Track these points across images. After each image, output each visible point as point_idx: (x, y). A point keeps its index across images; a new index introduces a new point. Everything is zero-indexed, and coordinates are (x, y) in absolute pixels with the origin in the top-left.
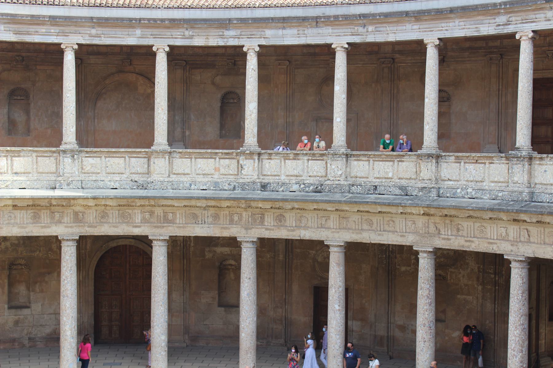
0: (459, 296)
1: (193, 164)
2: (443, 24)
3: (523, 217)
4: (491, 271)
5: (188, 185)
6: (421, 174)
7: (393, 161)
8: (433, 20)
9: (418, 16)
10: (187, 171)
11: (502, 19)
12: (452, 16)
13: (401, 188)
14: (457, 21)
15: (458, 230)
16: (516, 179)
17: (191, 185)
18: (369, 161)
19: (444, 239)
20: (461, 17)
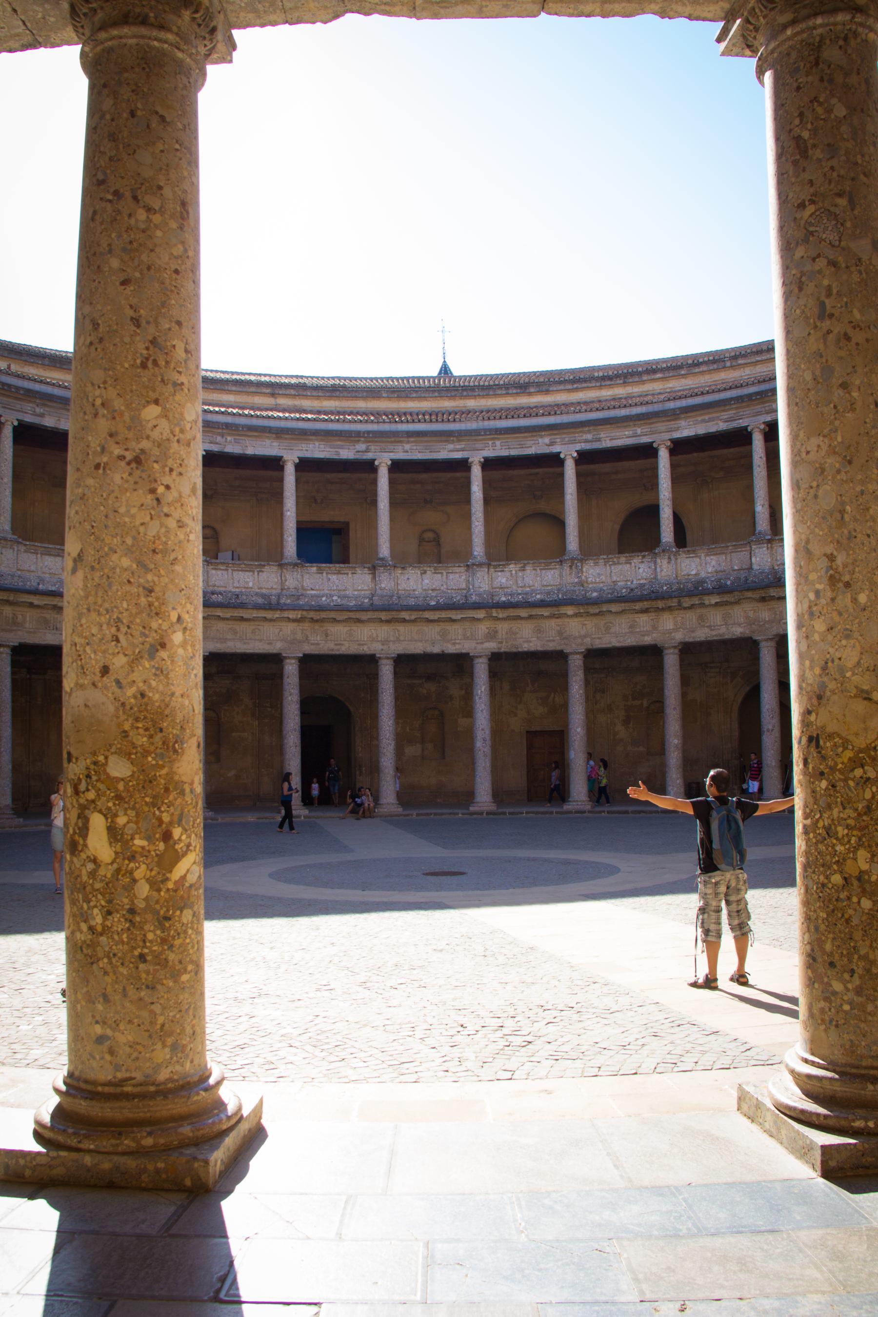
0: (234, 734)
1: (39, 560)
2: (304, 446)
3: (405, 615)
4: (268, 705)
5: (35, 584)
6: (287, 583)
7: (253, 572)
8: (292, 439)
9: (279, 433)
10: (33, 568)
11: (362, 447)
12: (314, 438)
13: (263, 596)
14: (317, 444)
15: (327, 635)
16: (383, 586)
17: (39, 584)
18: (227, 570)
19: (312, 644)
20: (322, 440)
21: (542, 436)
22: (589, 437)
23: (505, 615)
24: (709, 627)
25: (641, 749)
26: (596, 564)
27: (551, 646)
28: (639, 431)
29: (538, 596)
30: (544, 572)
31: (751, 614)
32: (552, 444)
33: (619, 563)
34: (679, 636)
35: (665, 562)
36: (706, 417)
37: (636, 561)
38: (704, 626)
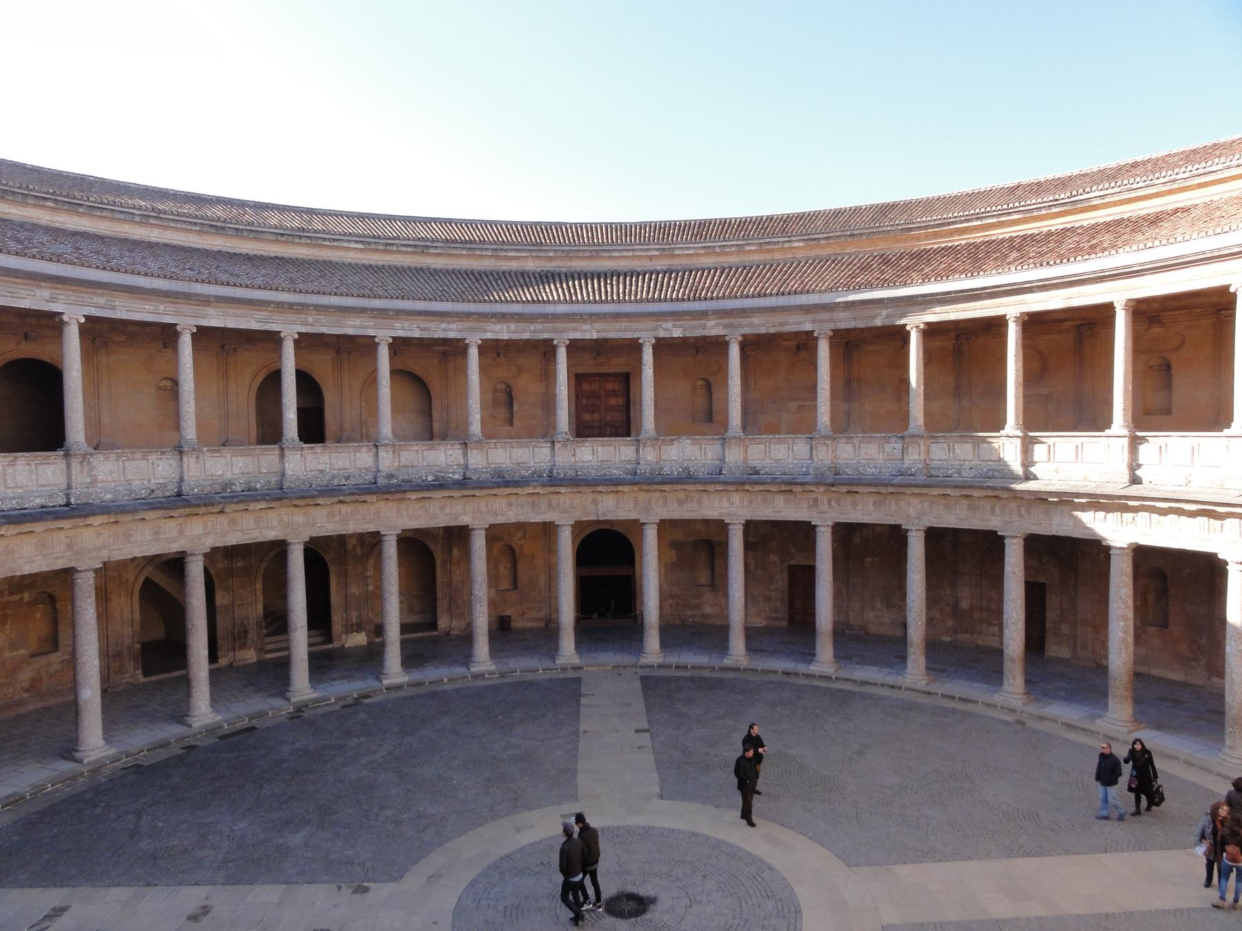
21: (39, 287)
22: (102, 301)
23: (15, 532)
24: (242, 531)
25: (22, 652)
26: (106, 459)
27: (60, 564)
28: (161, 307)
29: (38, 501)
30: (41, 468)
31: (285, 518)
32: (53, 300)
33: (134, 459)
34: (209, 542)
35: (193, 461)
36: (238, 312)
37: (153, 457)
38: (235, 531)
